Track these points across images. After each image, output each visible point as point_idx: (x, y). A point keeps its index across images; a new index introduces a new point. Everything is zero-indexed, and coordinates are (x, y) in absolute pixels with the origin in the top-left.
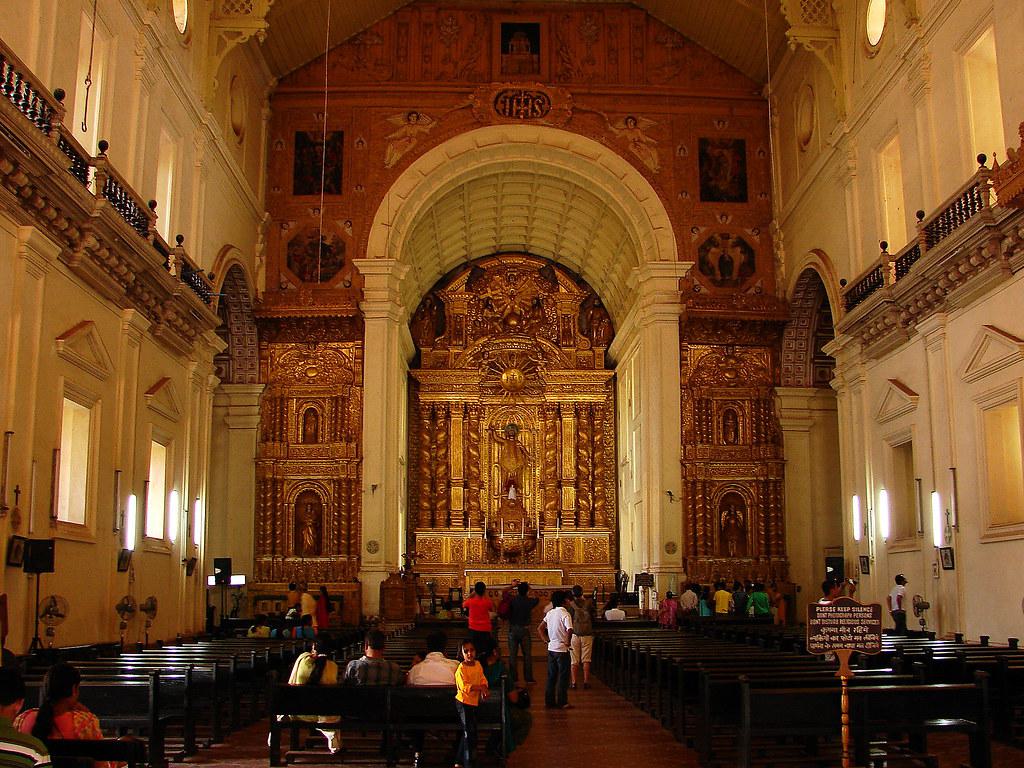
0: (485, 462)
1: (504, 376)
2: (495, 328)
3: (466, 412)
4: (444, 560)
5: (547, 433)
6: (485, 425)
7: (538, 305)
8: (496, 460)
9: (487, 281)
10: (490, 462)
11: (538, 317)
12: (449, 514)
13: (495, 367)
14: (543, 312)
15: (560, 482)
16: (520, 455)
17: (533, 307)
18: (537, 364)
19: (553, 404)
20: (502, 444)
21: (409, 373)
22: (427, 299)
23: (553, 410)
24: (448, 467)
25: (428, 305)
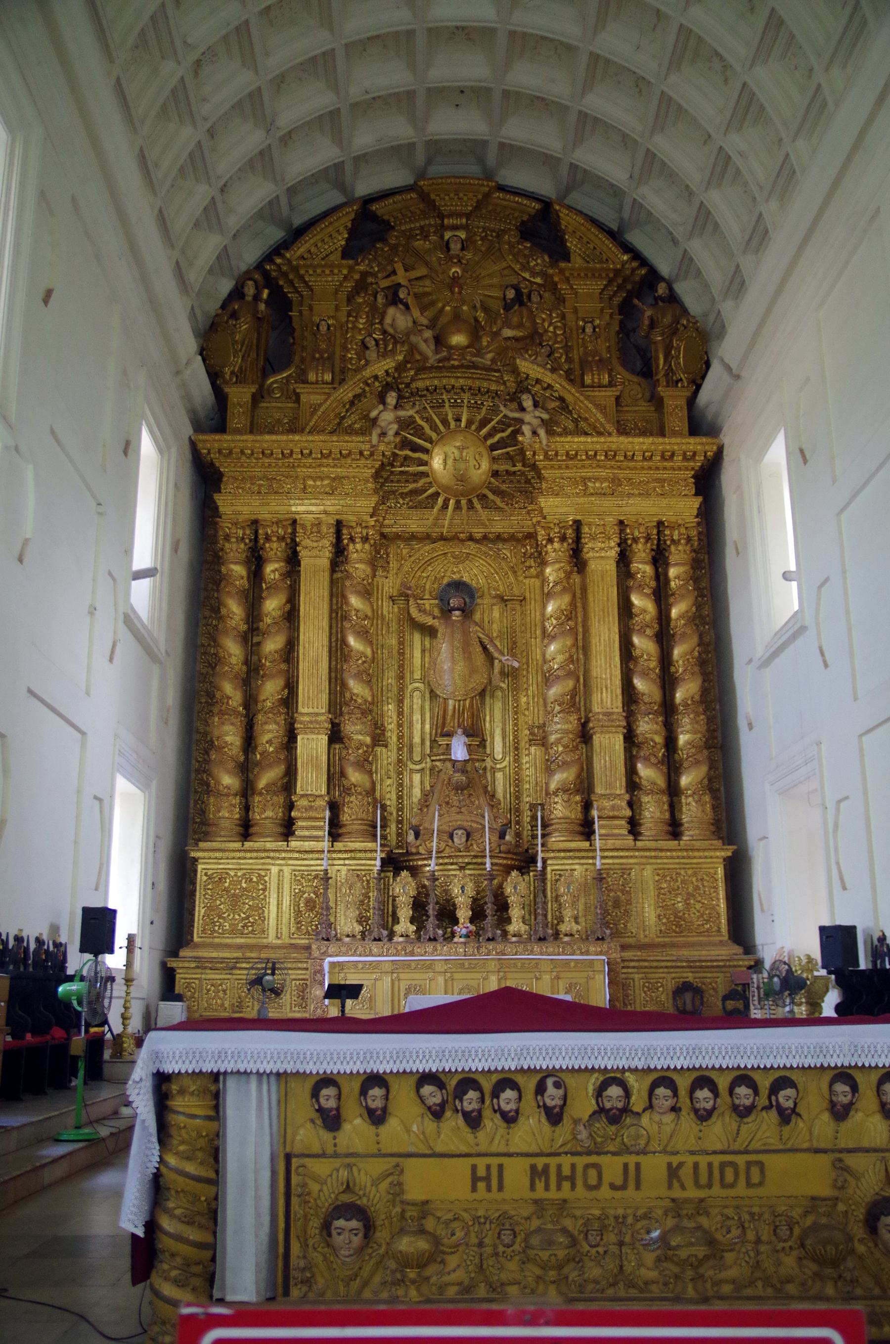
0: (390, 678)
1: (436, 462)
2: (413, 348)
3: (339, 552)
4: (272, 932)
5: (547, 596)
6: (389, 584)
7: (520, 299)
8: (417, 675)
9: (394, 248)
10: (401, 677)
11: (520, 326)
12: (291, 806)
13: (419, 432)
14: (532, 317)
15: (588, 720)
16: (479, 658)
17: (507, 307)
18: (521, 421)
19: (560, 524)
20: (430, 632)
21: (193, 444)
22: (250, 279)
23: (563, 539)
24: (291, 687)
25: (249, 298)
